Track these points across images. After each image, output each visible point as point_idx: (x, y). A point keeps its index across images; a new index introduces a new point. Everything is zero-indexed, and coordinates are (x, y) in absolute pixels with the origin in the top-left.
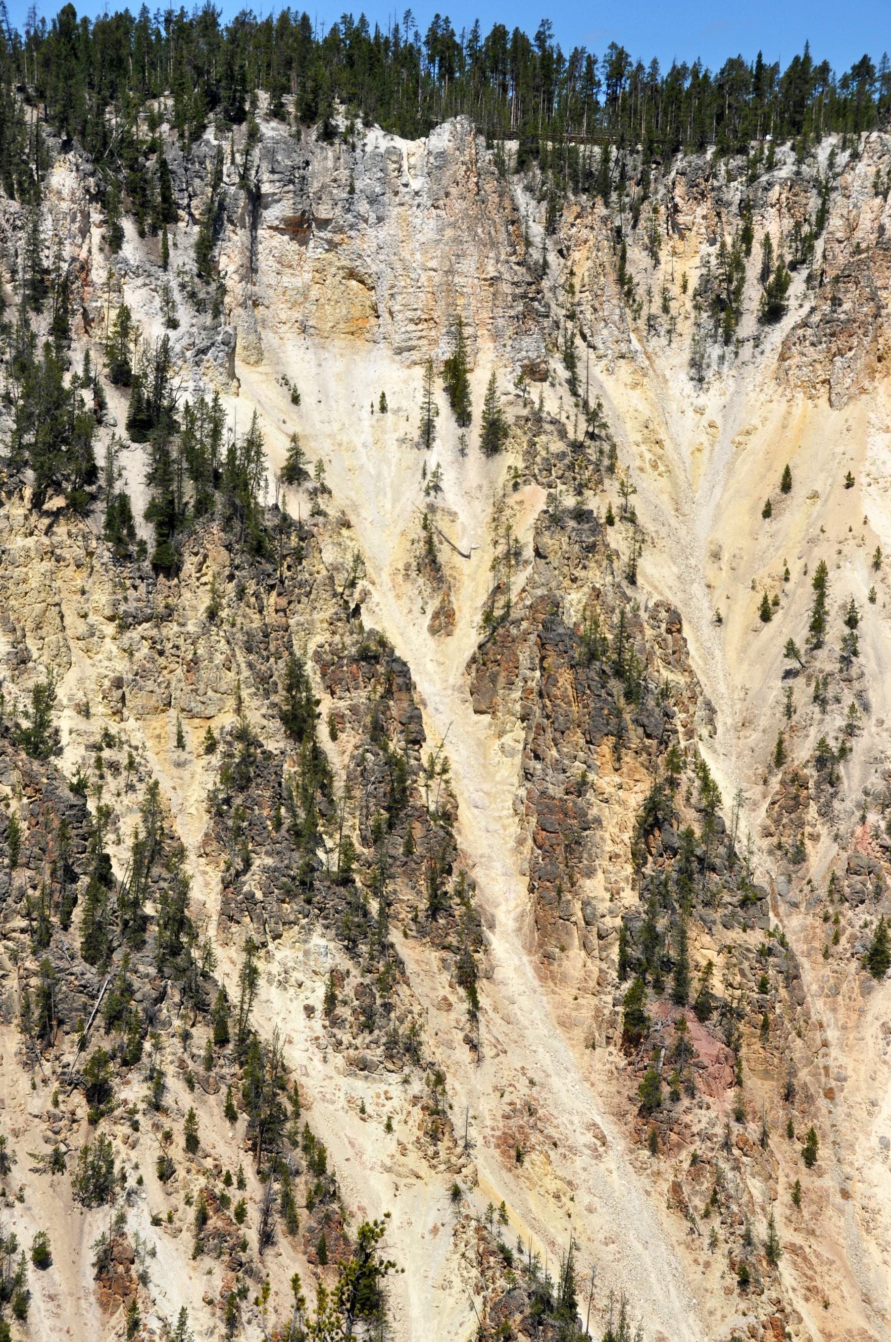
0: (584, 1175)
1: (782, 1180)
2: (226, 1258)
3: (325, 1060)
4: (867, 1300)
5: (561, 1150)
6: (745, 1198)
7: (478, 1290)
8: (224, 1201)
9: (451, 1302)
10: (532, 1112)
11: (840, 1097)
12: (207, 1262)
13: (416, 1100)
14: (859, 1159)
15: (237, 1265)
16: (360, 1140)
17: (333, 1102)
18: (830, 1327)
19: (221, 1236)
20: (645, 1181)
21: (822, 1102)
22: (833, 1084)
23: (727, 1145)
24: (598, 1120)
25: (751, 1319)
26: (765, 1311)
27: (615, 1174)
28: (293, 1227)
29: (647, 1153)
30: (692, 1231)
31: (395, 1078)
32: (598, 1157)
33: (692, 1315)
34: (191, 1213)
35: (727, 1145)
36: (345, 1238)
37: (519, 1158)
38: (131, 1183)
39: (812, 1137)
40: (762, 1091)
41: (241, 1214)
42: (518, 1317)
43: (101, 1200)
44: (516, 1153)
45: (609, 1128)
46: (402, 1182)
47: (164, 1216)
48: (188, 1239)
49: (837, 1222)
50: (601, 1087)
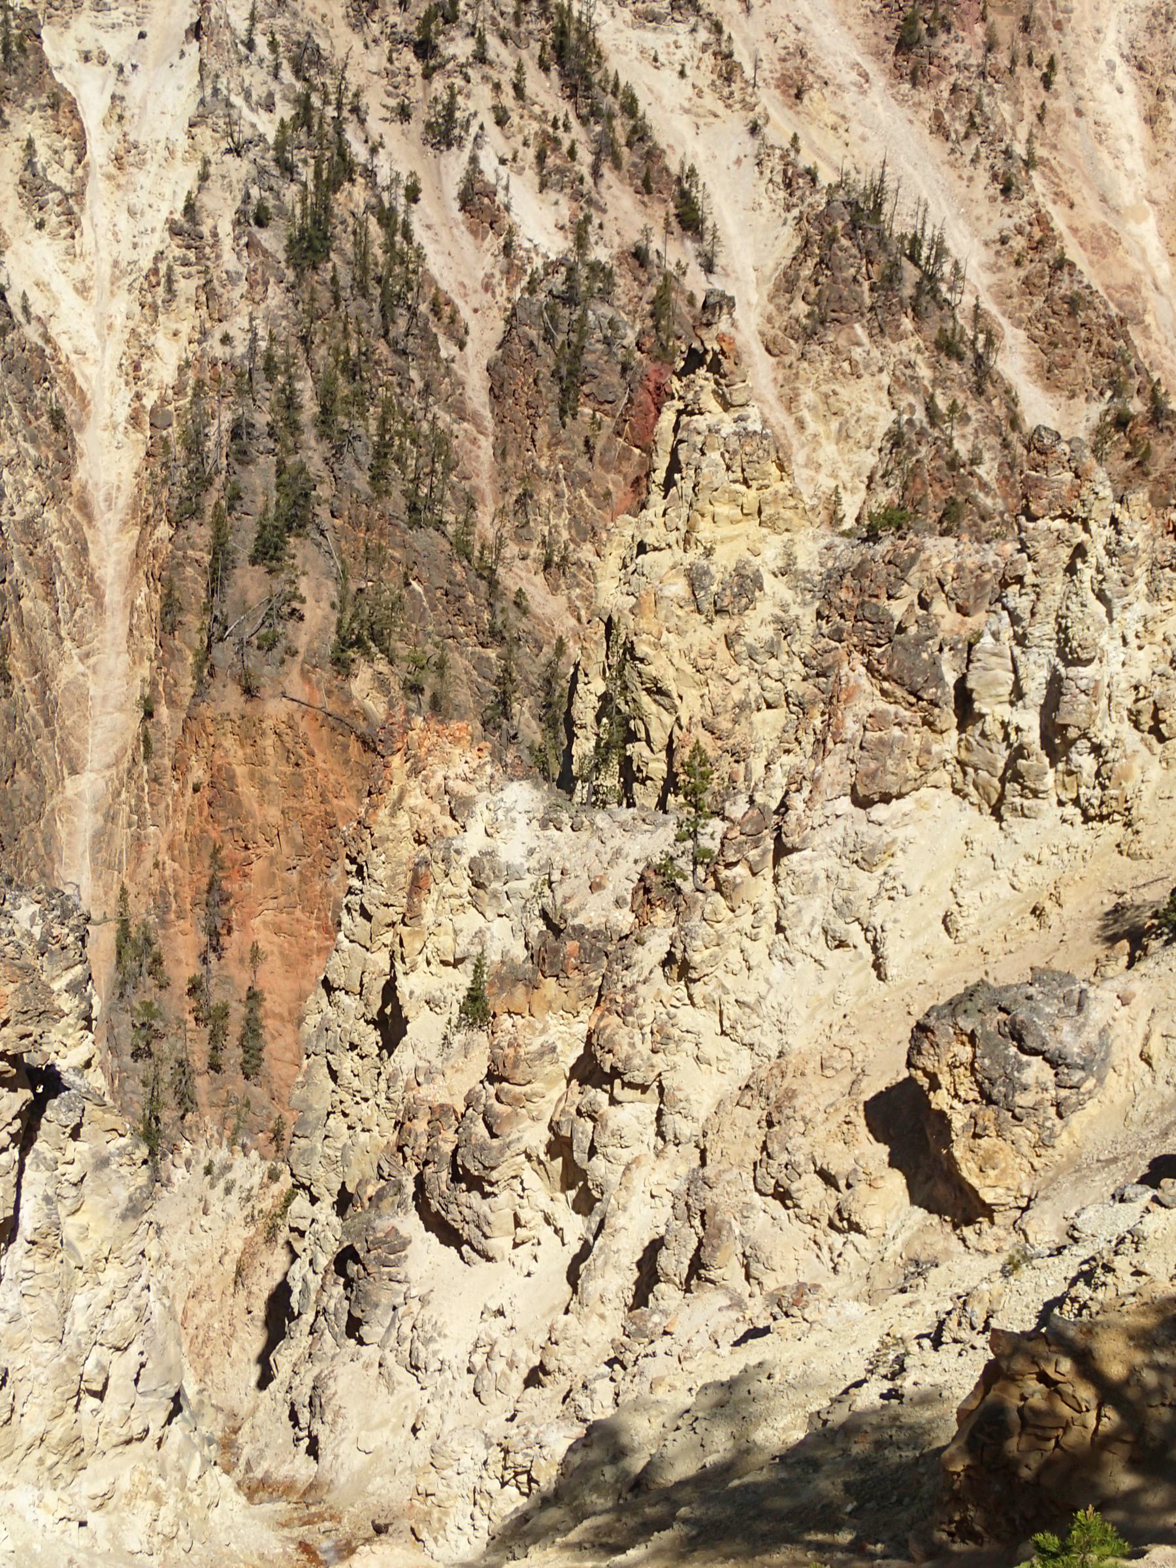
0: (853, 109)
1: (1027, 103)
2: (568, 191)
3: (613, 14)
4: (1104, 199)
5: (831, 88)
6: (998, 120)
7: (788, 209)
8: (557, 142)
9: (763, 220)
10: (803, 56)
11: (1067, 28)
12: (552, 195)
13: (705, 47)
14: (1088, 80)
15: (577, 196)
16: (657, 87)
17: (625, 53)
18: (1077, 223)
19: (560, 171)
20: (909, 113)
21: (1052, 33)
22: (1061, 16)
23: (983, 75)
24: (859, 60)
25: (1016, 219)
26: (1025, 214)
27: (880, 108)
28: (617, 165)
29: (908, 86)
30: (953, 151)
31: (682, 28)
32: (864, 93)
33: (961, 222)
34: (530, 154)
35: (983, 75)
36: (666, 169)
37: (798, 96)
38: (474, 129)
39: (1051, 65)
40: (1005, 25)
41: (572, 153)
42: (840, 224)
43: (449, 146)
44: (795, 92)
45: (870, 66)
46: (701, 122)
47: (509, 156)
48: (531, 176)
49: (1074, 137)
50: (858, 30)
